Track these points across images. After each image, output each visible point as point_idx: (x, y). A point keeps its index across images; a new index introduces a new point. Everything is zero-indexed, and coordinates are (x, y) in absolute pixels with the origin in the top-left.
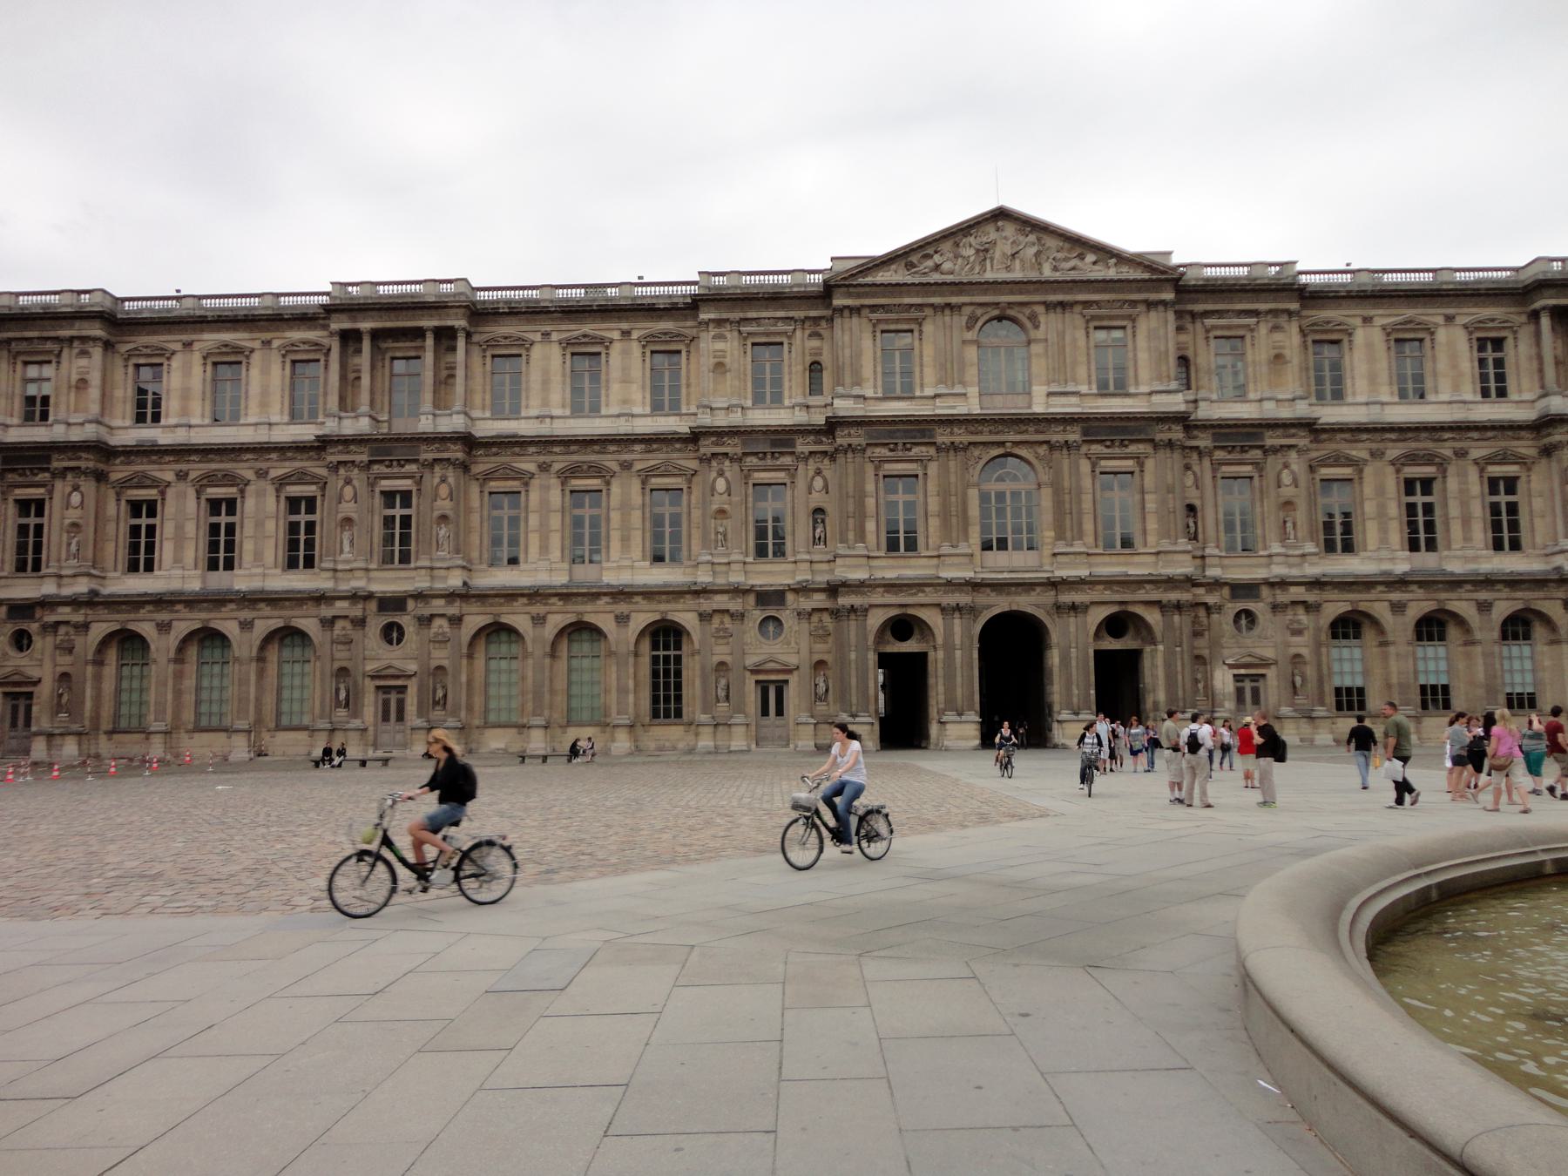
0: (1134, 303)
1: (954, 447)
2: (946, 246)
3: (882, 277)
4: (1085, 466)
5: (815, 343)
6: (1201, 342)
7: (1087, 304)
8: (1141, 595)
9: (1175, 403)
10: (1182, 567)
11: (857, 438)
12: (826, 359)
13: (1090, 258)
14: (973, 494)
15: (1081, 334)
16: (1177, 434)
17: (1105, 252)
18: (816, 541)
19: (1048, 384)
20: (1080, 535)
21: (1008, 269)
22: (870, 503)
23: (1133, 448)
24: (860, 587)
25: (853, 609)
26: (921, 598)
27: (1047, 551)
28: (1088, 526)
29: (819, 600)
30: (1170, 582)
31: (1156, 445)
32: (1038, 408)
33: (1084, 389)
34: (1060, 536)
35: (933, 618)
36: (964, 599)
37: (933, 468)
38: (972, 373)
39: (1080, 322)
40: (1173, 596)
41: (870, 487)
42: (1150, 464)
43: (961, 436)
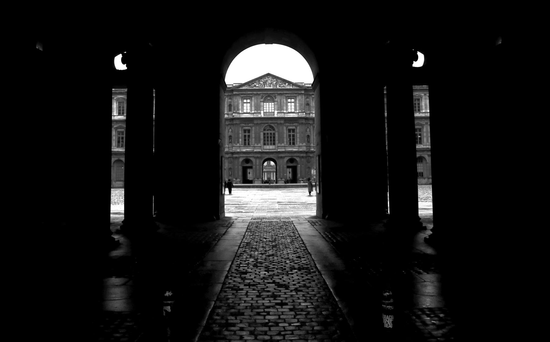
0: (296, 94)
1: (257, 124)
2: (257, 81)
3: (244, 88)
4: (285, 128)
5: (230, 100)
6: (311, 101)
7: (286, 94)
8: (295, 155)
9: (304, 115)
10: (304, 149)
11: (238, 122)
12: (232, 104)
13: (287, 84)
14: (262, 134)
15: (285, 100)
16: (304, 121)
17: (290, 83)
18: (230, 143)
19: (278, 110)
20: (283, 142)
21: (270, 86)
22: (241, 135)
23: (294, 124)
24: (238, 153)
25: (236, 157)
26: (250, 155)
27: (276, 145)
28: (285, 140)
29: (230, 155)
30: (301, 152)
31: (300, 124)
32: (276, 116)
33: (285, 111)
34: (279, 143)
35: (253, 159)
36: (259, 155)
37: (253, 128)
38: (262, 108)
39: (285, 97)
40: (302, 155)
41: (240, 132)
42: (298, 128)
43: (259, 122)
